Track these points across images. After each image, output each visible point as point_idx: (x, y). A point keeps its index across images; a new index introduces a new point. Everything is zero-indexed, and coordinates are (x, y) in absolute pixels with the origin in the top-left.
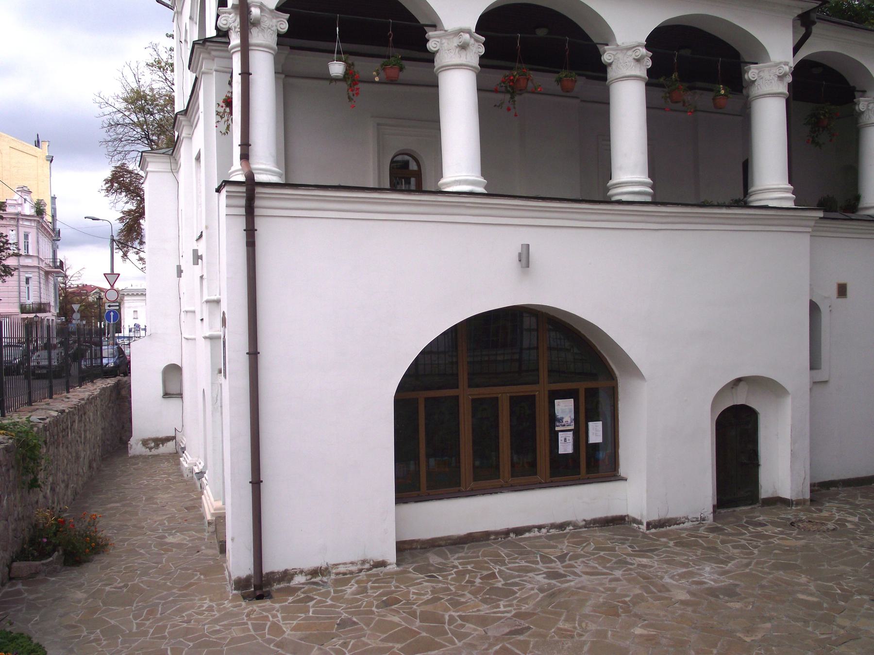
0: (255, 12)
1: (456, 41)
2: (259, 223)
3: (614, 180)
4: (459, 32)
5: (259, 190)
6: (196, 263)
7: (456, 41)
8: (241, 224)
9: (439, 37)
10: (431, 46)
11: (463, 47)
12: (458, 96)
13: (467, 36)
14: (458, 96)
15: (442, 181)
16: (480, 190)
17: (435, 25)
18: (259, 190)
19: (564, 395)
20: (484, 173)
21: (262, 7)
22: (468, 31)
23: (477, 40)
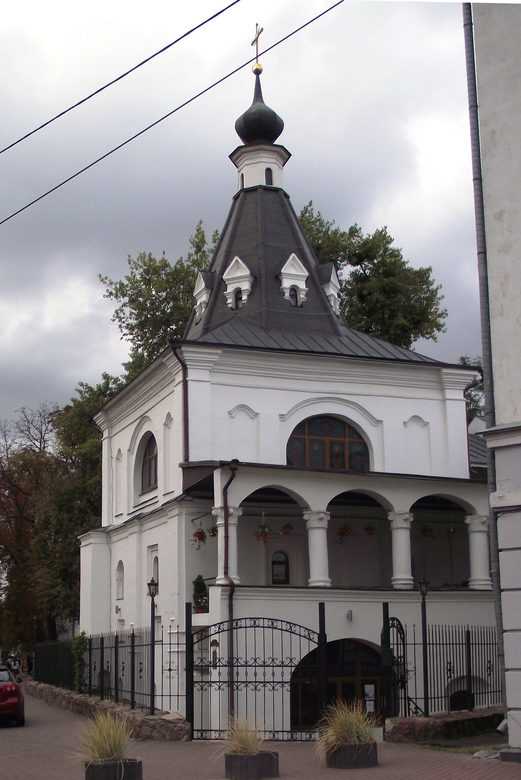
0: (231, 510)
1: (317, 517)
2: (234, 602)
3: (394, 578)
4: (319, 513)
5: (236, 588)
6: (117, 612)
7: (317, 517)
8: (227, 603)
9: (310, 514)
10: (305, 517)
11: (321, 519)
12: (318, 542)
13: (322, 515)
14: (318, 542)
15: (309, 580)
16: (329, 585)
17: (307, 508)
18: (236, 588)
19: (370, 683)
20: (330, 576)
21: (234, 508)
22: (323, 513)
23: (326, 514)
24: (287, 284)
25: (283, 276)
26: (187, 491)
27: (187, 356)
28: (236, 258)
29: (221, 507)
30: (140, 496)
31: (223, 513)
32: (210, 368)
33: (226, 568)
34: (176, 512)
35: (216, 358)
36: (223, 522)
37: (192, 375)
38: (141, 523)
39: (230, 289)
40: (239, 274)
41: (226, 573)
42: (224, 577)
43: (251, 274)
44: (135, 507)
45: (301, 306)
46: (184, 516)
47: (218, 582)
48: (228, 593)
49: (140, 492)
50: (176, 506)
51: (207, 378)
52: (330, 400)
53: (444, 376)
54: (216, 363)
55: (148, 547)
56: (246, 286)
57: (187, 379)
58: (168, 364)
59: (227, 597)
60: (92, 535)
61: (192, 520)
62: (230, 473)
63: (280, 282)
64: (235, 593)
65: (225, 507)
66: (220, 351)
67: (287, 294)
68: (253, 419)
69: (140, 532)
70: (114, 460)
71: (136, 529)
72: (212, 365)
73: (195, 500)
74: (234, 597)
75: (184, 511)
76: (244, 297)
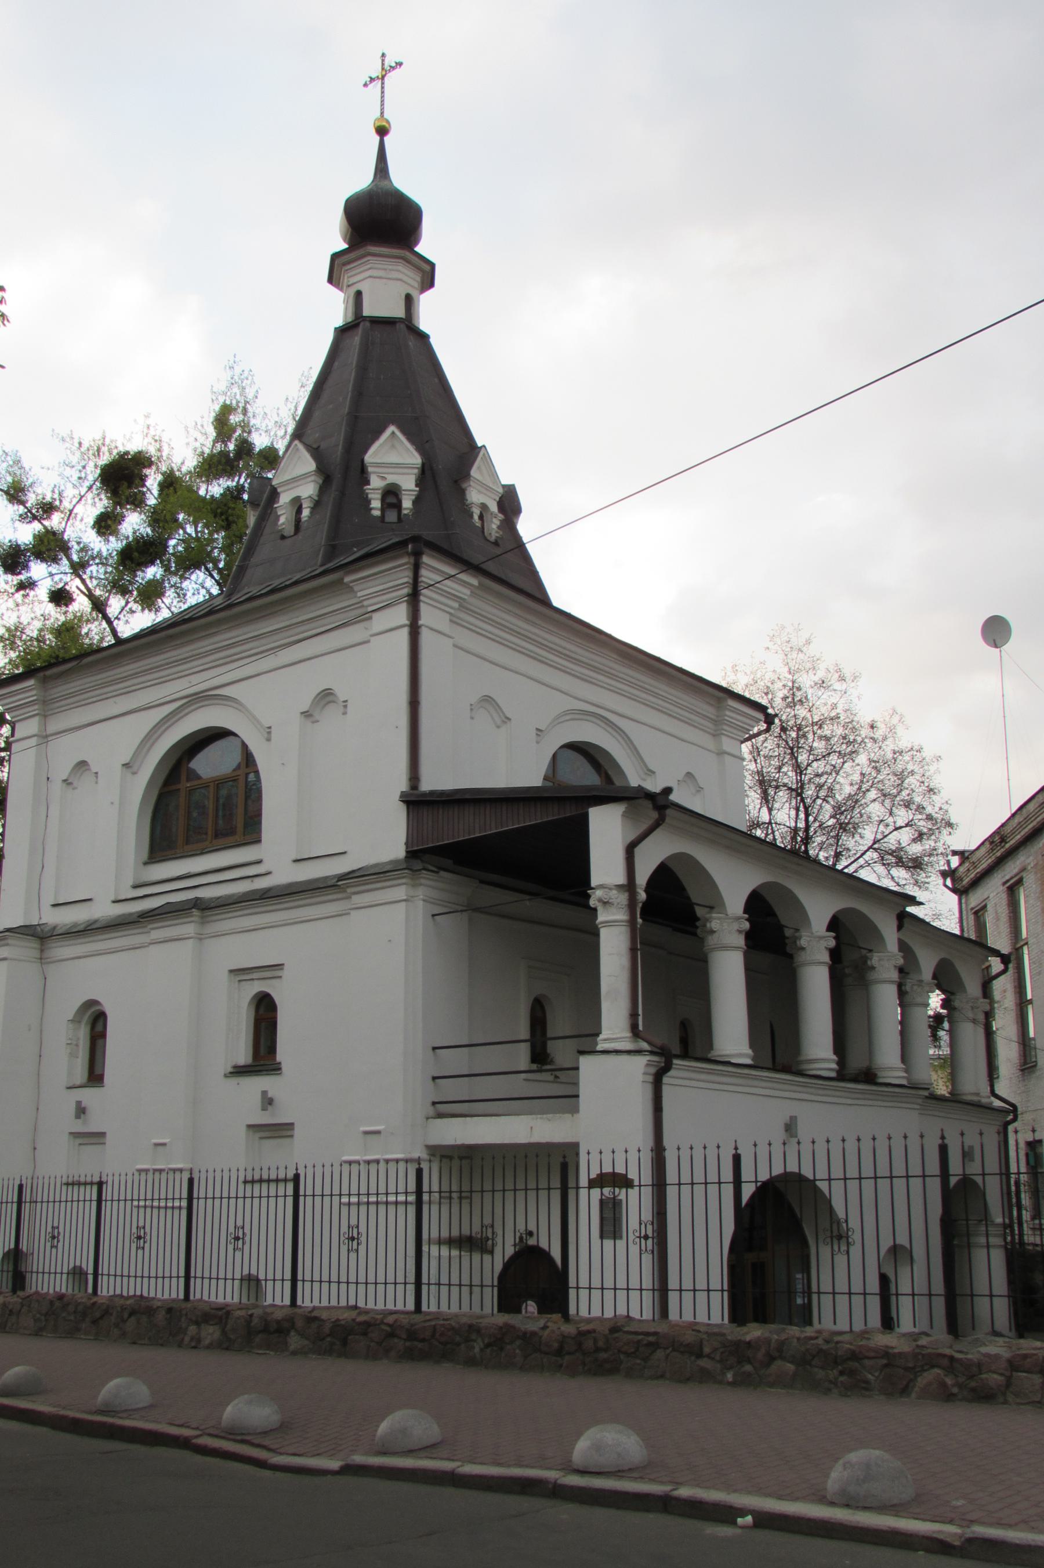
4: (738, 919)
8: (649, 1090)
9: (719, 919)
24: (475, 496)
25: (472, 483)
26: (413, 854)
27: (427, 576)
28: (392, 428)
29: (619, 887)
30: (145, 864)
31: (623, 898)
32: (452, 611)
33: (634, 1015)
34: (400, 892)
35: (465, 592)
36: (622, 916)
37: (428, 616)
38: (202, 917)
39: (376, 483)
40: (393, 458)
41: (634, 1028)
42: (629, 1034)
43: (423, 465)
44: (136, 887)
45: (496, 543)
46: (421, 902)
47: (599, 1048)
48: (653, 1070)
49: (145, 855)
50: (404, 881)
51: (447, 631)
52: (588, 718)
53: (728, 713)
54: (463, 606)
55: (231, 971)
56: (408, 483)
57: (420, 622)
58: (356, 588)
59: (650, 1078)
60: (10, 941)
61: (433, 916)
62: (655, 815)
63: (462, 493)
64: (672, 1073)
65: (630, 886)
66: (474, 582)
67: (476, 517)
68: (498, 727)
69: (200, 938)
70: (57, 786)
71: (188, 928)
72: (456, 605)
73: (442, 873)
74: (665, 1080)
75: (421, 892)
76: (407, 504)
